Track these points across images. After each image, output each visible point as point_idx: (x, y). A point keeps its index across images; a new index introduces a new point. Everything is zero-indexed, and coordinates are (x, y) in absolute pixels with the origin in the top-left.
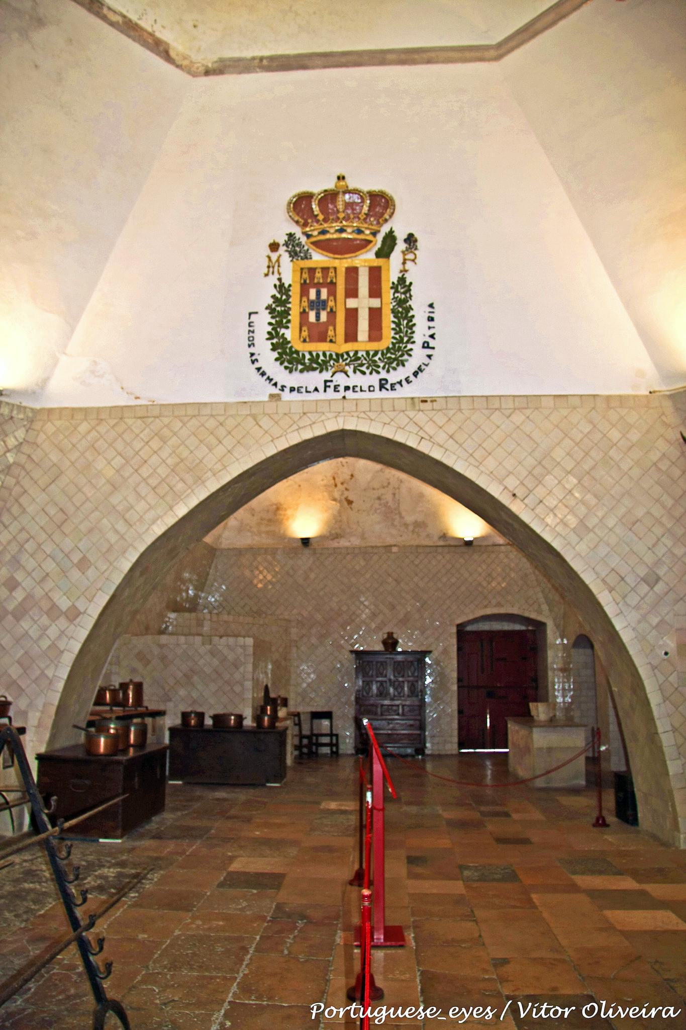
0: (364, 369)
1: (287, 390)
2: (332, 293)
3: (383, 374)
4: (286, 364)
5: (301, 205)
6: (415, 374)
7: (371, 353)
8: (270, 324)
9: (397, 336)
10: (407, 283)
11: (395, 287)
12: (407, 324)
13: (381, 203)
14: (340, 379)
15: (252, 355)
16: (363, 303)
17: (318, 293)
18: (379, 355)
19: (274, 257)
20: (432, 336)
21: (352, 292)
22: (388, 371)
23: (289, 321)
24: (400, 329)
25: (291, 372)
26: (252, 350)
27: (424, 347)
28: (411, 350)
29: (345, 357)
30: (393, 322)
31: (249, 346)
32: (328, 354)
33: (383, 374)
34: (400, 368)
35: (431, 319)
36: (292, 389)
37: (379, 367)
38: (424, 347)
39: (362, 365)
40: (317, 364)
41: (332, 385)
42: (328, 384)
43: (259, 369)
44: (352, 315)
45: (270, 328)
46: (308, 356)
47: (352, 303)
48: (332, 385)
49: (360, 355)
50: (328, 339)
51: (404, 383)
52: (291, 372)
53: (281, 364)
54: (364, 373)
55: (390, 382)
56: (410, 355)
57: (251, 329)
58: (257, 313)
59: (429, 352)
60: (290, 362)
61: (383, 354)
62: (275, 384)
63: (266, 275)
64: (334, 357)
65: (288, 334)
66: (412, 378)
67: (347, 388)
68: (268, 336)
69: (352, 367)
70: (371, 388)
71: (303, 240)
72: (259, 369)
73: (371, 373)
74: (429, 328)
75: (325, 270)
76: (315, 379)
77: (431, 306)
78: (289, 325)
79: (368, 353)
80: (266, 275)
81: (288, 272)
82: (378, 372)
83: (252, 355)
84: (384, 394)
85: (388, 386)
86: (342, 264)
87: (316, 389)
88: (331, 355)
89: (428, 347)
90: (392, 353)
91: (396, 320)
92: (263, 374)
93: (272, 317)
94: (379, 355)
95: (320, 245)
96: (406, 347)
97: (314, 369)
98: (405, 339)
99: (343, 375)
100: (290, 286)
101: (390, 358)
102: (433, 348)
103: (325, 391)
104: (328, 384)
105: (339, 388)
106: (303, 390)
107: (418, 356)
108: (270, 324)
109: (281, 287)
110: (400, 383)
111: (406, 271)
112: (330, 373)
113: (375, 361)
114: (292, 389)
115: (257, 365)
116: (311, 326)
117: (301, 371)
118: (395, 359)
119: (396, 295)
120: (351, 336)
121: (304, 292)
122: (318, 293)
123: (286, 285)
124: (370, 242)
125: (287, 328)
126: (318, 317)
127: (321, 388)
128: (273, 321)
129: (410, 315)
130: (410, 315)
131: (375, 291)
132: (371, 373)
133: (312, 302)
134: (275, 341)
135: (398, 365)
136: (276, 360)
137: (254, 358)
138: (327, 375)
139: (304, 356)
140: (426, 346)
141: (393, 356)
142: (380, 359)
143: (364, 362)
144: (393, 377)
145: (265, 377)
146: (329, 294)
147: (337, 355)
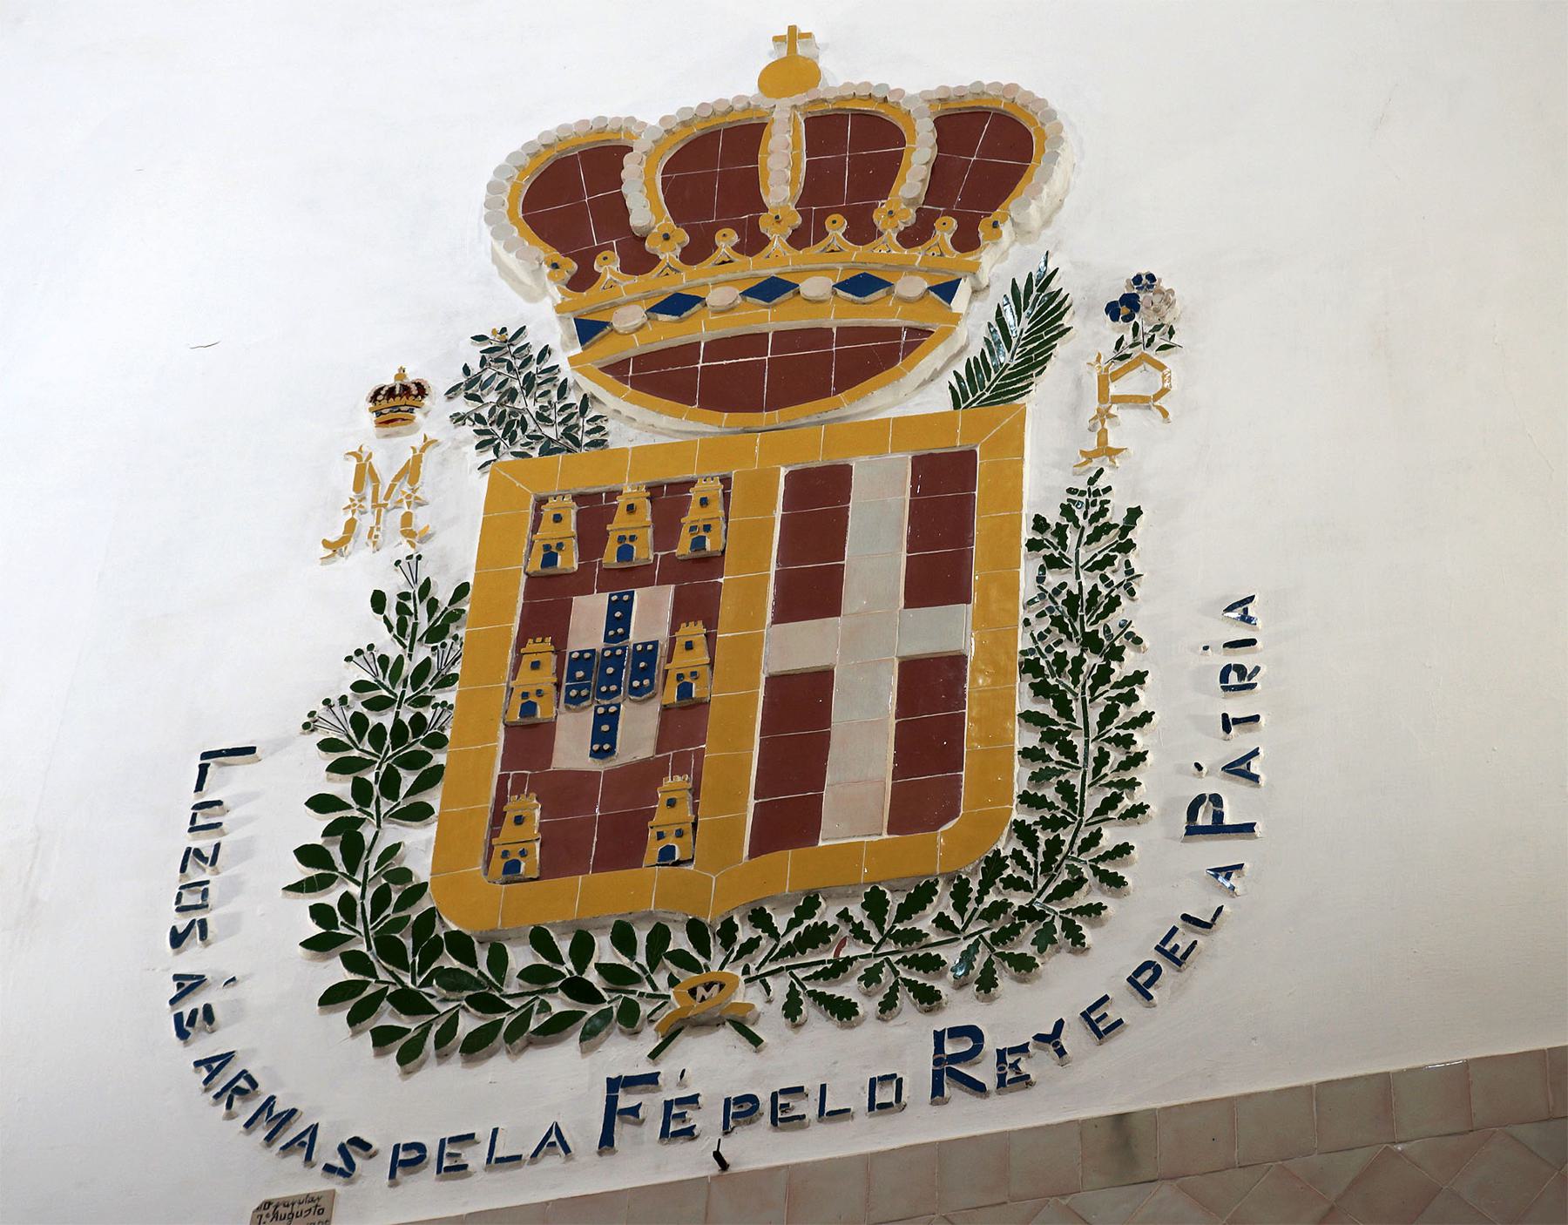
0: (847, 989)
1: (373, 1172)
2: (697, 605)
3: (961, 1008)
4: (387, 1017)
5: (568, 199)
6: (1143, 981)
7: (895, 901)
8: (320, 803)
9: (1050, 793)
10: (1116, 516)
11: (1048, 540)
12: (1109, 715)
13: (989, 151)
14: (710, 1066)
15: (188, 984)
16: (867, 642)
17: (619, 618)
18: (943, 902)
19: (389, 454)
20: (1239, 769)
21: (811, 591)
22: (987, 983)
23: (431, 778)
24: (1068, 750)
25: (410, 1056)
26: (192, 960)
27: (1193, 830)
28: (1123, 850)
29: (743, 935)
30: (1028, 717)
31: (177, 939)
32: (642, 936)
33: (961, 1008)
34: (1057, 966)
35: (1237, 679)
36: (408, 1159)
37: (932, 964)
38: (1193, 830)
39: (838, 969)
40: (578, 997)
41: (651, 1104)
42: (625, 1101)
43: (213, 1065)
44: (801, 704)
45: (313, 828)
46: (521, 957)
47: (797, 646)
48: (651, 1104)
49: (827, 914)
50: (654, 848)
51: (1075, 1037)
52: (410, 1056)
53: (353, 1020)
54: (843, 1011)
55: (991, 1045)
56: (1116, 882)
57: (205, 843)
58: (251, 750)
59: (1222, 851)
60: (409, 1002)
61: (960, 896)
62: (307, 1142)
63: (336, 548)
64: (680, 941)
65: (418, 847)
66: (1124, 1006)
67: (741, 1110)
68: (302, 872)
69: (780, 986)
70: (884, 1096)
71: (565, 355)
72: (213, 1065)
73: (888, 1005)
74: (1227, 724)
75: (669, 499)
76: (556, 1082)
77: (1241, 607)
78: (434, 797)
79: (875, 904)
80: (336, 548)
81: (459, 512)
82: (928, 998)
83: (188, 984)
84: (965, 1120)
85: (984, 1071)
86: (763, 451)
87: (554, 1141)
88: (660, 936)
89: (1218, 827)
90: (1015, 884)
91: (1047, 708)
92: (239, 1089)
93: (334, 768)
94: (943, 902)
95: (658, 376)
96: (1095, 838)
97: (556, 1027)
98: (1093, 800)
99: (727, 1034)
100: (462, 591)
101: (1000, 908)
102: (1248, 828)
103: (607, 1140)
104: (625, 1101)
105: (694, 1118)
106: (475, 1157)
107: (1162, 872)
108: (320, 803)
109: (419, 613)
110: (1052, 1039)
111: (1112, 453)
112: (650, 1038)
113: (916, 936)
114: (408, 1159)
115: (207, 1045)
116: (565, 792)
117: (476, 1046)
118: (1028, 913)
119: (1053, 579)
120: (789, 817)
121: (546, 610)
122: (619, 618)
123: (443, 594)
124: (919, 335)
125: (419, 813)
126: (604, 738)
127: (585, 1125)
128: (341, 787)
129: (1119, 671)
130: (1119, 671)
131: (937, 575)
132: (888, 1005)
133: (585, 661)
134: (331, 898)
135: (1045, 940)
136: (331, 998)
137: (196, 1002)
138: (624, 1054)
139: (498, 960)
140: (1204, 819)
141: (1018, 900)
142: (942, 922)
143: (849, 951)
144: (1011, 1014)
145: (246, 1110)
146: (681, 614)
147: (697, 931)
